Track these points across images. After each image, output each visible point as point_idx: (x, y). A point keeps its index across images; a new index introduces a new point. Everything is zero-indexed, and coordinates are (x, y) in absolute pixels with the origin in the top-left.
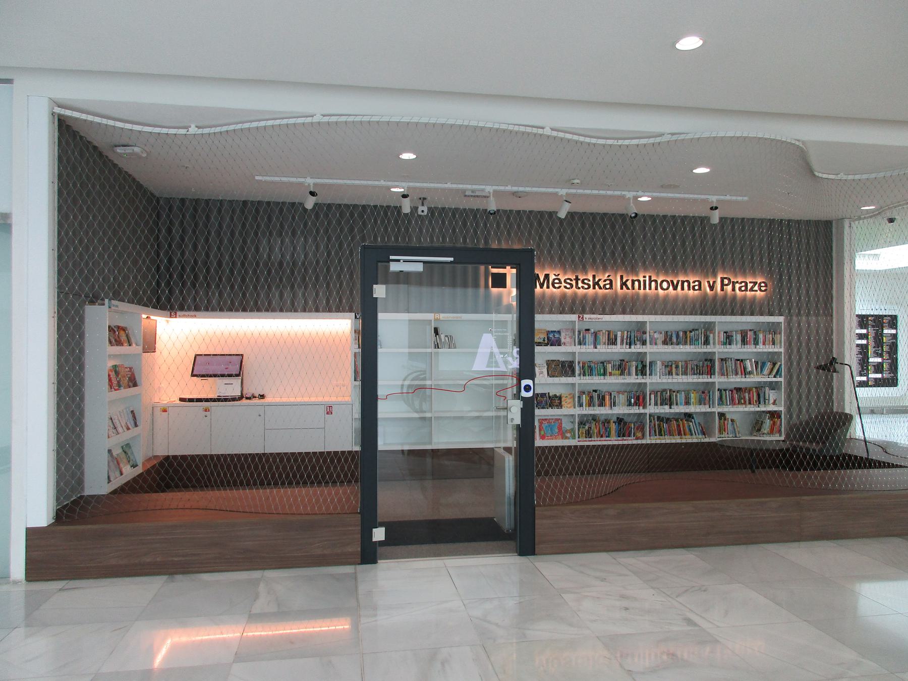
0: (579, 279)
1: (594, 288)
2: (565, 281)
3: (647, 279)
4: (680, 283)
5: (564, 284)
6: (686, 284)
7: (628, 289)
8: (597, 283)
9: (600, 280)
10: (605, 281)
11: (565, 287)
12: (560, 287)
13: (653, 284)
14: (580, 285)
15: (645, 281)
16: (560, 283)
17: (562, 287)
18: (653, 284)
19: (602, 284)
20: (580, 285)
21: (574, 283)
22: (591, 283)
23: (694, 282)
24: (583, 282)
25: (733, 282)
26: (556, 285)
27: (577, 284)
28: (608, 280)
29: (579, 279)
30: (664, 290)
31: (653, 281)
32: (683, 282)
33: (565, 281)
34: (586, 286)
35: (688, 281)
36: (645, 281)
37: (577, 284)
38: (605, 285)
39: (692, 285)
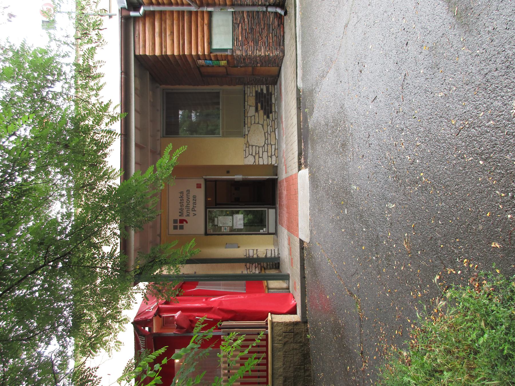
14: (182, 202)
19: (182, 195)
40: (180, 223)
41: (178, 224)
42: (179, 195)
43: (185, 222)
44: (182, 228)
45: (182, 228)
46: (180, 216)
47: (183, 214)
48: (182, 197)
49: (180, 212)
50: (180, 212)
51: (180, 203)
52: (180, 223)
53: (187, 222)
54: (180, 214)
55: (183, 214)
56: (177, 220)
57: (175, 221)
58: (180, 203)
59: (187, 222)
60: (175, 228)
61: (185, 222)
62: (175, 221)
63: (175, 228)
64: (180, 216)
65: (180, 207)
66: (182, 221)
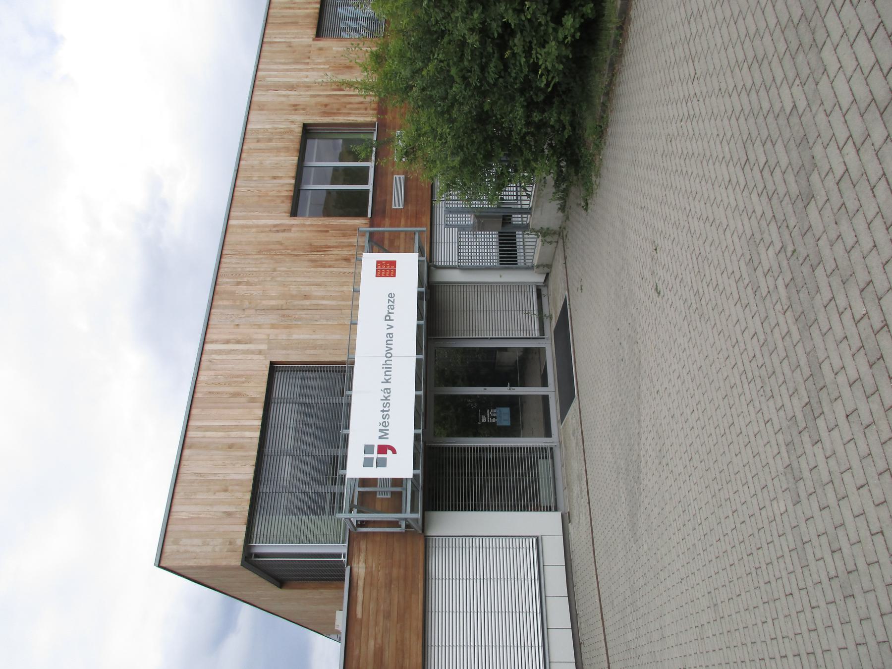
1: (389, 400)
3: (384, 366)
5: (386, 420)
6: (389, 342)
7: (389, 379)
8: (386, 398)
9: (384, 396)
10: (385, 393)
13: (388, 362)
14: (386, 409)
15: (386, 368)
18: (388, 362)
19: (386, 395)
20: (386, 409)
21: (385, 413)
22: (386, 402)
26: (387, 424)
31: (386, 362)
32: (387, 344)
33: (384, 419)
34: (388, 405)
36: (386, 368)
38: (388, 393)
40: (379, 452)
41: (375, 455)
42: (381, 395)
43: (389, 452)
44: (382, 463)
45: (382, 463)
46: (380, 438)
47: (387, 434)
48: (386, 399)
49: (380, 431)
50: (380, 431)
51: (383, 411)
52: (379, 452)
53: (394, 452)
55: (387, 434)
56: (373, 446)
57: (368, 449)
58: (383, 411)
59: (394, 452)
60: (368, 463)
61: (389, 452)
62: (368, 449)
63: (368, 463)
64: (380, 438)
66: (383, 449)
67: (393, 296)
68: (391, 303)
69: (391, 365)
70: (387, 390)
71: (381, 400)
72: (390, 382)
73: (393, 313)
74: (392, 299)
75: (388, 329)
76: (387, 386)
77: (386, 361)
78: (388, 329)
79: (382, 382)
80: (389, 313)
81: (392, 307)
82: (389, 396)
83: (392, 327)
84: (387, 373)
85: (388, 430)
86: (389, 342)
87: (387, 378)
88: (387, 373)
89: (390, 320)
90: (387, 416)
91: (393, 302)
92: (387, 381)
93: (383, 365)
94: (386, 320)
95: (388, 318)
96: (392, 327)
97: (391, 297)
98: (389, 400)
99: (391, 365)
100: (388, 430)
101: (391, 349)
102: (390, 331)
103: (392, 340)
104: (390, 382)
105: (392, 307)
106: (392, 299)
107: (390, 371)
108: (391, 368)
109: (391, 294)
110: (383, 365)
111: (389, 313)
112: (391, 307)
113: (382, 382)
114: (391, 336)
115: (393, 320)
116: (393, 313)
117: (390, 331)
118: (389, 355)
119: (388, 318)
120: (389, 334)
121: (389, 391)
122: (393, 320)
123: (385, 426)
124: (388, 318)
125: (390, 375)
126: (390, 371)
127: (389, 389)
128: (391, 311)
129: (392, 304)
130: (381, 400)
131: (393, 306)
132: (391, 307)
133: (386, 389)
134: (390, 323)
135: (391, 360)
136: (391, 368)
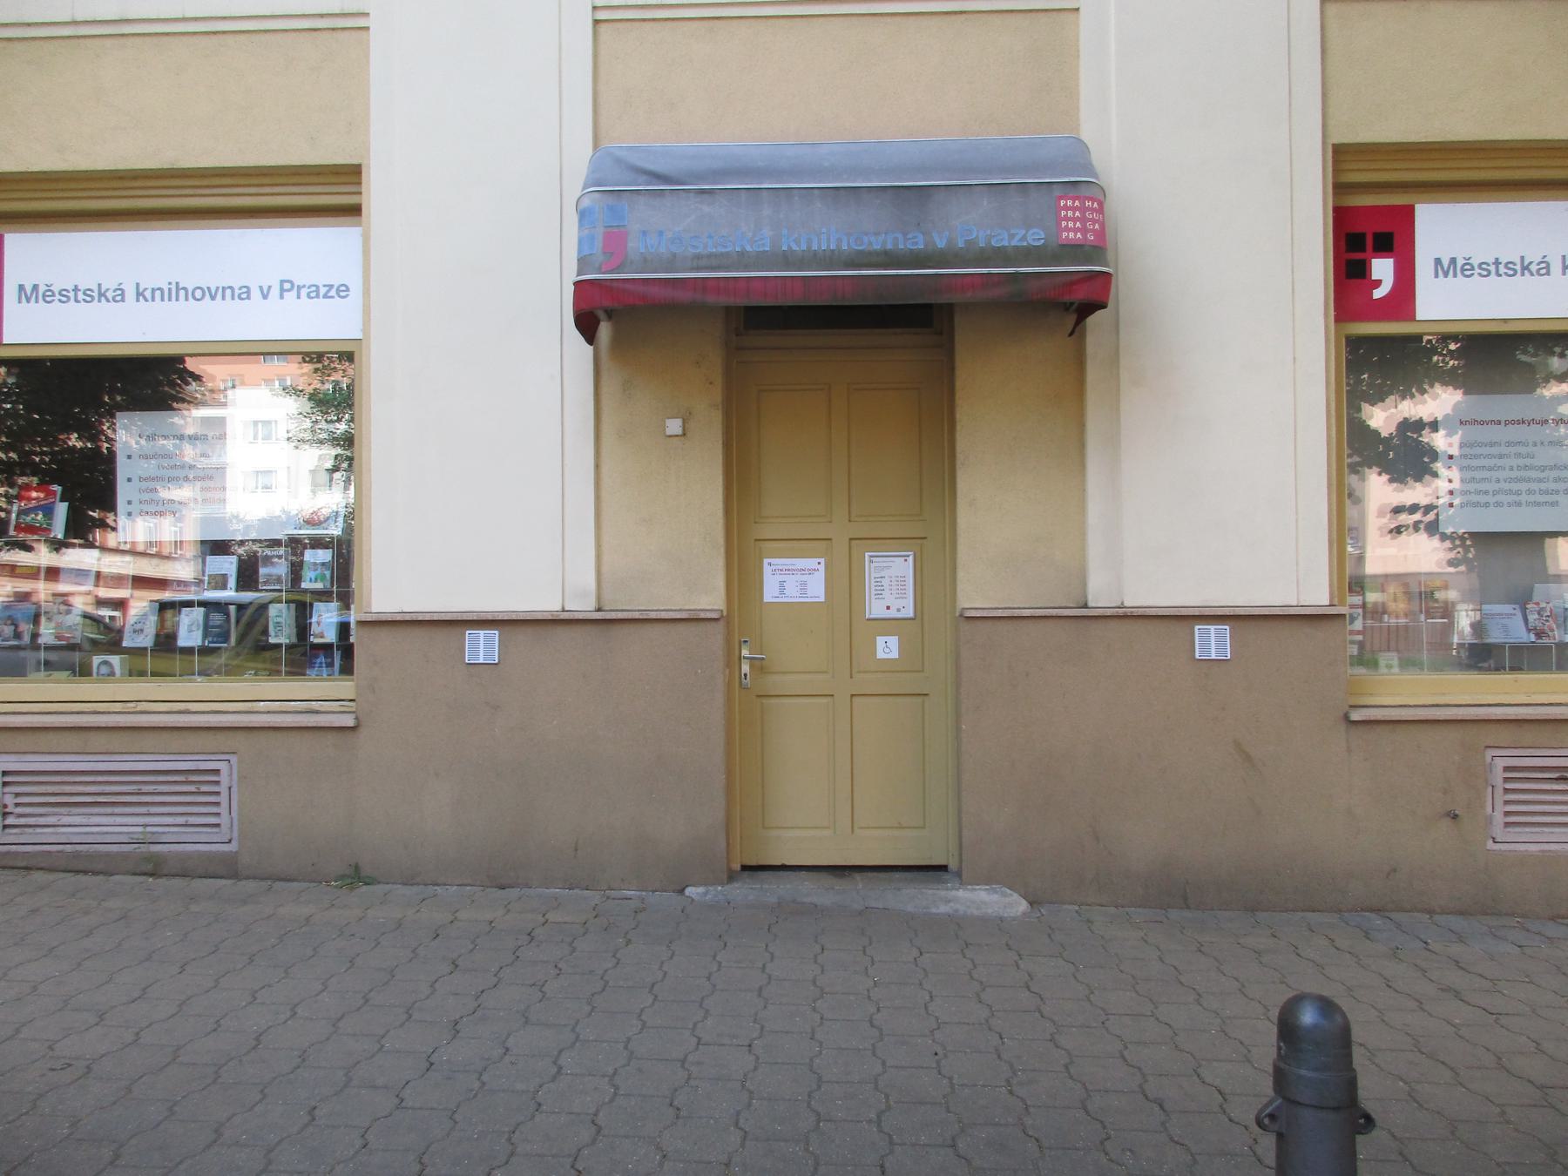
0: (80, 290)
2: (60, 294)
4: (220, 290)
5: (58, 297)
6: (228, 292)
10: (114, 291)
11: (60, 300)
12: (54, 300)
16: (53, 295)
17: (57, 302)
19: (110, 295)
20: (81, 296)
23: (240, 288)
24: (85, 294)
25: (298, 286)
27: (76, 295)
28: (120, 289)
29: (80, 290)
30: (198, 300)
35: (230, 287)
37: (76, 295)
39: (237, 292)
42: (109, 284)
46: (21, 287)
47: (28, 300)
48: (102, 295)
49: (35, 287)
50: (35, 287)
51: (76, 289)
54: (29, 290)
55: (28, 300)
58: (76, 289)
64: (21, 287)
65: (56, 289)
67: (342, 294)
68: (323, 291)
69: (177, 300)
70: (121, 295)
71: (99, 285)
72: (138, 300)
73: (299, 297)
74: (333, 293)
75: (261, 288)
76: (130, 294)
77: (185, 289)
78: (261, 288)
79: (138, 285)
80: (299, 288)
81: (313, 295)
82: (108, 301)
83: (265, 297)
84: (158, 293)
85: (37, 302)
86: (228, 292)
87: (148, 294)
88: (158, 293)
89: (282, 290)
90: (64, 299)
91: (325, 296)
92: (140, 294)
93: (177, 283)
94: (282, 282)
95: (286, 286)
96: (265, 297)
97: (338, 291)
98: (99, 301)
99: (177, 300)
100: (37, 302)
101: (213, 298)
102: (256, 294)
103: (233, 298)
104: (138, 300)
105: (313, 295)
106: (333, 293)
107: (162, 300)
108: (170, 300)
109: (348, 290)
110: (177, 283)
111: (299, 288)
112: (315, 292)
113: (138, 285)
114: (244, 296)
115: (282, 297)
116: (299, 297)
117: (256, 294)
118: (198, 294)
119: (287, 286)
120: (248, 292)
121: (119, 298)
122: (282, 297)
123: (44, 296)
124: (286, 286)
125: (153, 300)
126: (162, 300)
127: (123, 300)
128: (304, 292)
129: (321, 294)
130: (99, 285)
131: (318, 296)
132: (315, 292)
133: (123, 295)
134: (275, 291)
135: (187, 299)
136: (170, 300)
